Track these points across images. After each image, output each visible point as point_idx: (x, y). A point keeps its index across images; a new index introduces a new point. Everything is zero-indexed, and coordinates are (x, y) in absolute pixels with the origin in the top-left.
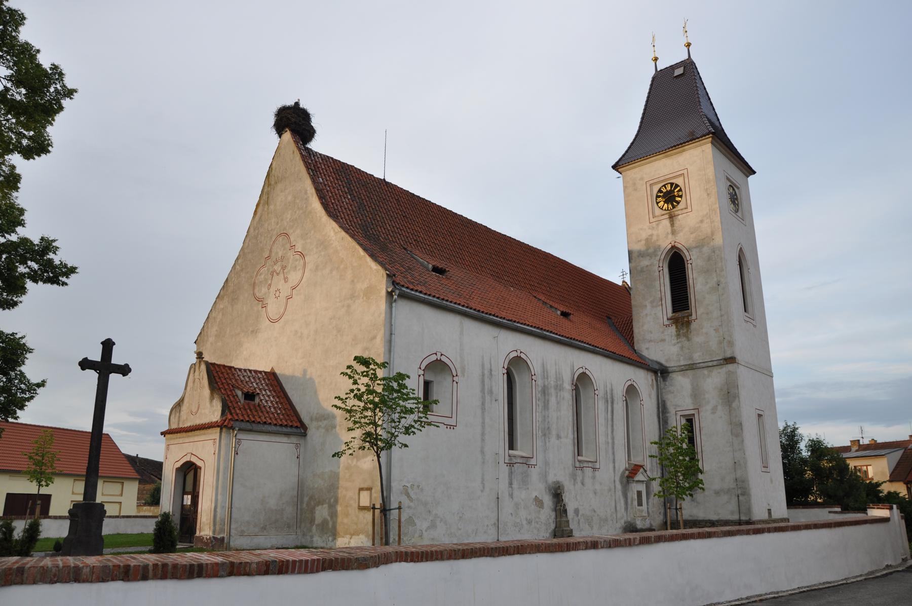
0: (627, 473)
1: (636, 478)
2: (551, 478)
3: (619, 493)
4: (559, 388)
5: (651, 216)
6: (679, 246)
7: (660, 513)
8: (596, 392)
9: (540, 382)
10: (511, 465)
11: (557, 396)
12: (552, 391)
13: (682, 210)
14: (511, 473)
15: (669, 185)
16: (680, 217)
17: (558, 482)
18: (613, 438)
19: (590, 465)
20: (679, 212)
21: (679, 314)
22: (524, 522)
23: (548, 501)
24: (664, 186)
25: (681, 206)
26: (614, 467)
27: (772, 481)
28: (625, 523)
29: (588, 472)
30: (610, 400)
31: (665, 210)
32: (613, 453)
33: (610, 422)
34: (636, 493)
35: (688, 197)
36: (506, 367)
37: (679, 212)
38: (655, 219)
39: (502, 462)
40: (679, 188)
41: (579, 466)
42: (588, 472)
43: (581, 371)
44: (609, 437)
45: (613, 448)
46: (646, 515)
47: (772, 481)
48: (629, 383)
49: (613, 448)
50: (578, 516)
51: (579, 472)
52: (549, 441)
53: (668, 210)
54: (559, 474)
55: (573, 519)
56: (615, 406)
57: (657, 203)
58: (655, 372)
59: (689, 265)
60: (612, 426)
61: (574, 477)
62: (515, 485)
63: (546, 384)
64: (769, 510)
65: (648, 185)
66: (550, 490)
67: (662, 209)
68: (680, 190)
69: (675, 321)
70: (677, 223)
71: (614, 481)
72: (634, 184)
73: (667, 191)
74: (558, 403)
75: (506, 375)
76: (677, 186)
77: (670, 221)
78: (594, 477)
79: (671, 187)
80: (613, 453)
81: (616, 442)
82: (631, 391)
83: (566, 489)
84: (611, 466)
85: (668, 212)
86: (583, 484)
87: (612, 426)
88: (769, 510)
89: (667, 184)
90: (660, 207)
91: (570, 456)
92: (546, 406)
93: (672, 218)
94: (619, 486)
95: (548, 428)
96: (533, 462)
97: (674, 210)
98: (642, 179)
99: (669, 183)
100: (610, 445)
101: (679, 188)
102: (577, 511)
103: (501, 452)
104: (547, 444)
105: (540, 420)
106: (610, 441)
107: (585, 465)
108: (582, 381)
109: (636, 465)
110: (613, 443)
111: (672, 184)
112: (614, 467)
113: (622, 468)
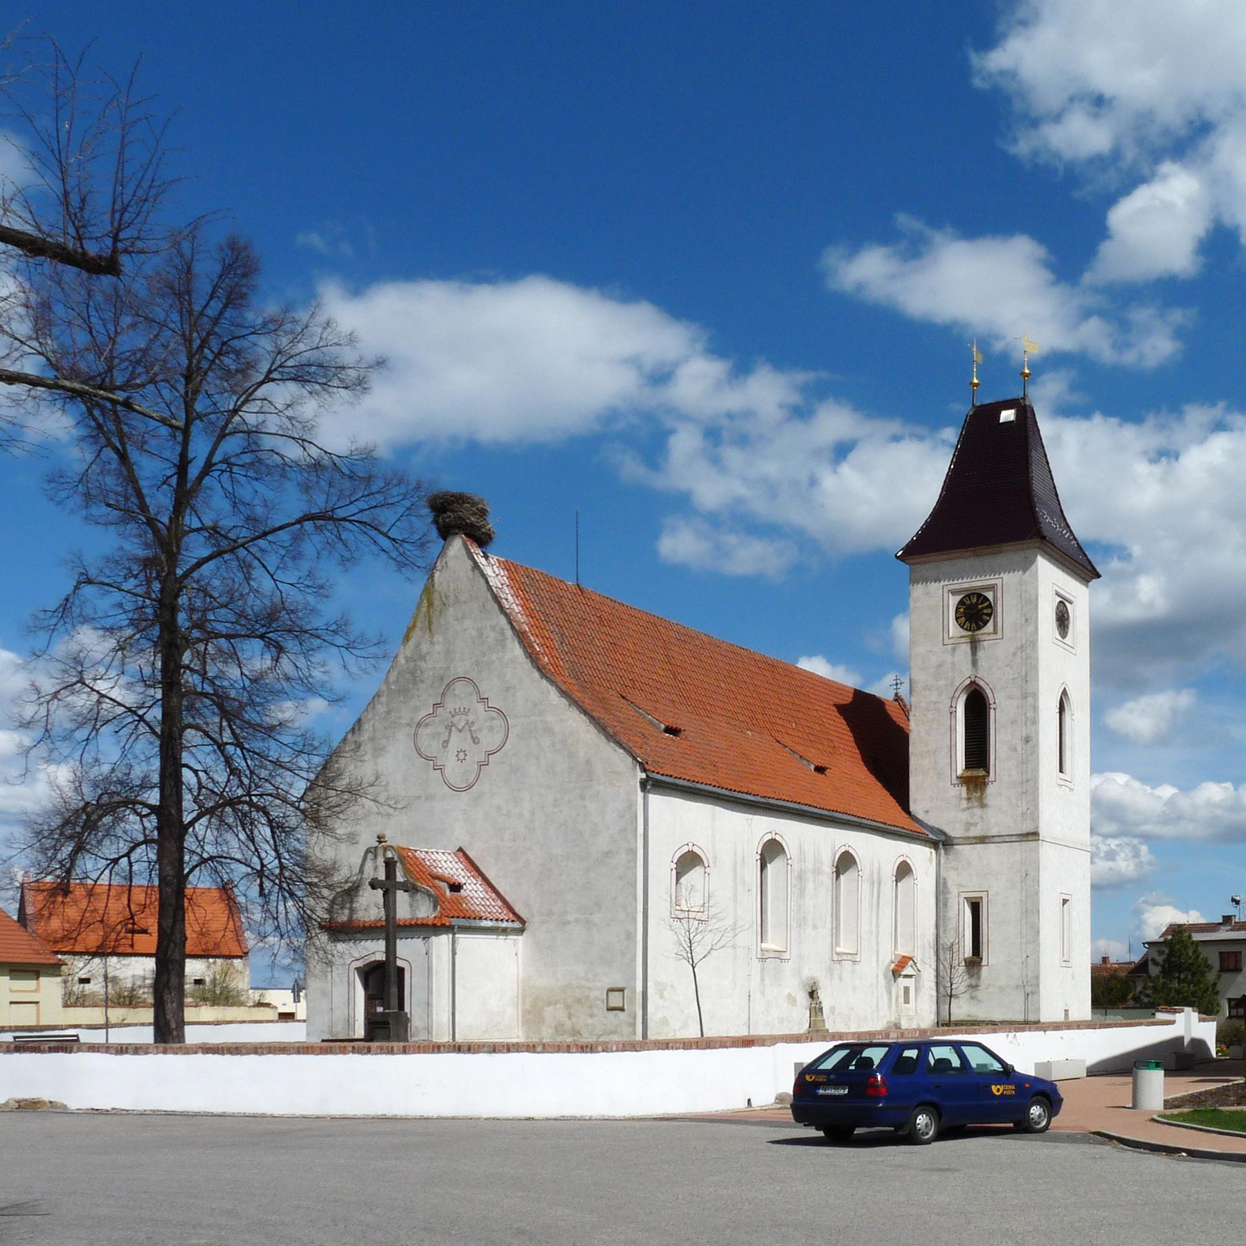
0: (893, 966)
1: (904, 973)
2: (806, 973)
3: (883, 990)
4: (817, 871)
6: (981, 683)
7: (931, 1012)
8: (860, 873)
9: (796, 867)
10: (763, 959)
11: (815, 881)
12: (810, 876)
13: (989, 634)
14: (763, 969)
17: (813, 978)
18: (878, 926)
19: (849, 957)
21: (969, 773)
22: (776, 1022)
23: (803, 999)
24: (968, 596)
26: (878, 960)
27: (1073, 978)
28: (888, 1023)
29: (847, 965)
30: (877, 883)
32: (877, 944)
33: (875, 908)
34: (902, 988)
35: (999, 619)
36: (759, 852)
39: (754, 958)
41: (838, 959)
42: (847, 965)
43: (843, 849)
44: (874, 924)
45: (877, 937)
46: (914, 1014)
47: (1073, 978)
48: (901, 859)
49: (877, 937)
50: (834, 1014)
51: (837, 966)
52: (804, 933)
53: (970, 630)
54: (814, 969)
55: (829, 1017)
56: (882, 888)
58: (935, 845)
59: (992, 712)
60: (878, 912)
61: (830, 971)
62: (767, 982)
63: (803, 868)
64: (1066, 1011)
66: (804, 987)
67: (962, 627)
69: (965, 780)
70: (980, 654)
71: (877, 976)
73: (972, 604)
74: (815, 889)
75: (759, 861)
76: (986, 599)
78: (853, 972)
80: (877, 944)
81: (881, 930)
82: (904, 870)
83: (821, 984)
84: (874, 959)
85: (970, 633)
86: (840, 980)
87: (878, 912)
88: (1066, 1011)
89: (973, 594)
91: (827, 948)
92: (802, 893)
93: (974, 645)
94: (882, 981)
95: (804, 918)
96: (786, 956)
97: (982, 631)
100: (874, 935)
102: (833, 1009)
103: (754, 947)
104: (802, 935)
105: (796, 909)
106: (874, 929)
107: (844, 957)
108: (845, 862)
109: (903, 957)
110: (878, 933)
111: (979, 595)
112: (878, 960)
113: (888, 961)
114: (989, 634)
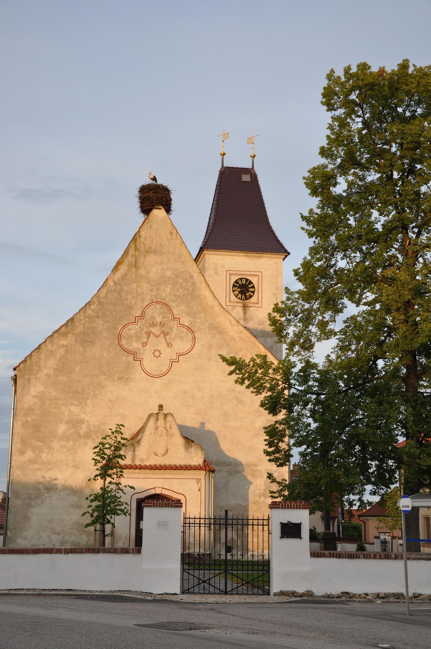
5: (228, 300)
13: (254, 303)
15: (245, 280)
16: (251, 308)
20: (252, 305)
25: (253, 300)
31: (239, 299)
37: (252, 305)
38: (230, 304)
40: (252, 285)
57: (233, 291)
65: (228, 273)
67: (236, 297)
68: (253, 287)
72: (216, 269)
77: (243, 310)
79: (246, 282)
89: (243, 278)
90: (235, 295)
93: (245, 307)
98: (223, 266)
99: (245, 278)
101: (252, 285)
111: (247, 280)
114: (254, 303)
